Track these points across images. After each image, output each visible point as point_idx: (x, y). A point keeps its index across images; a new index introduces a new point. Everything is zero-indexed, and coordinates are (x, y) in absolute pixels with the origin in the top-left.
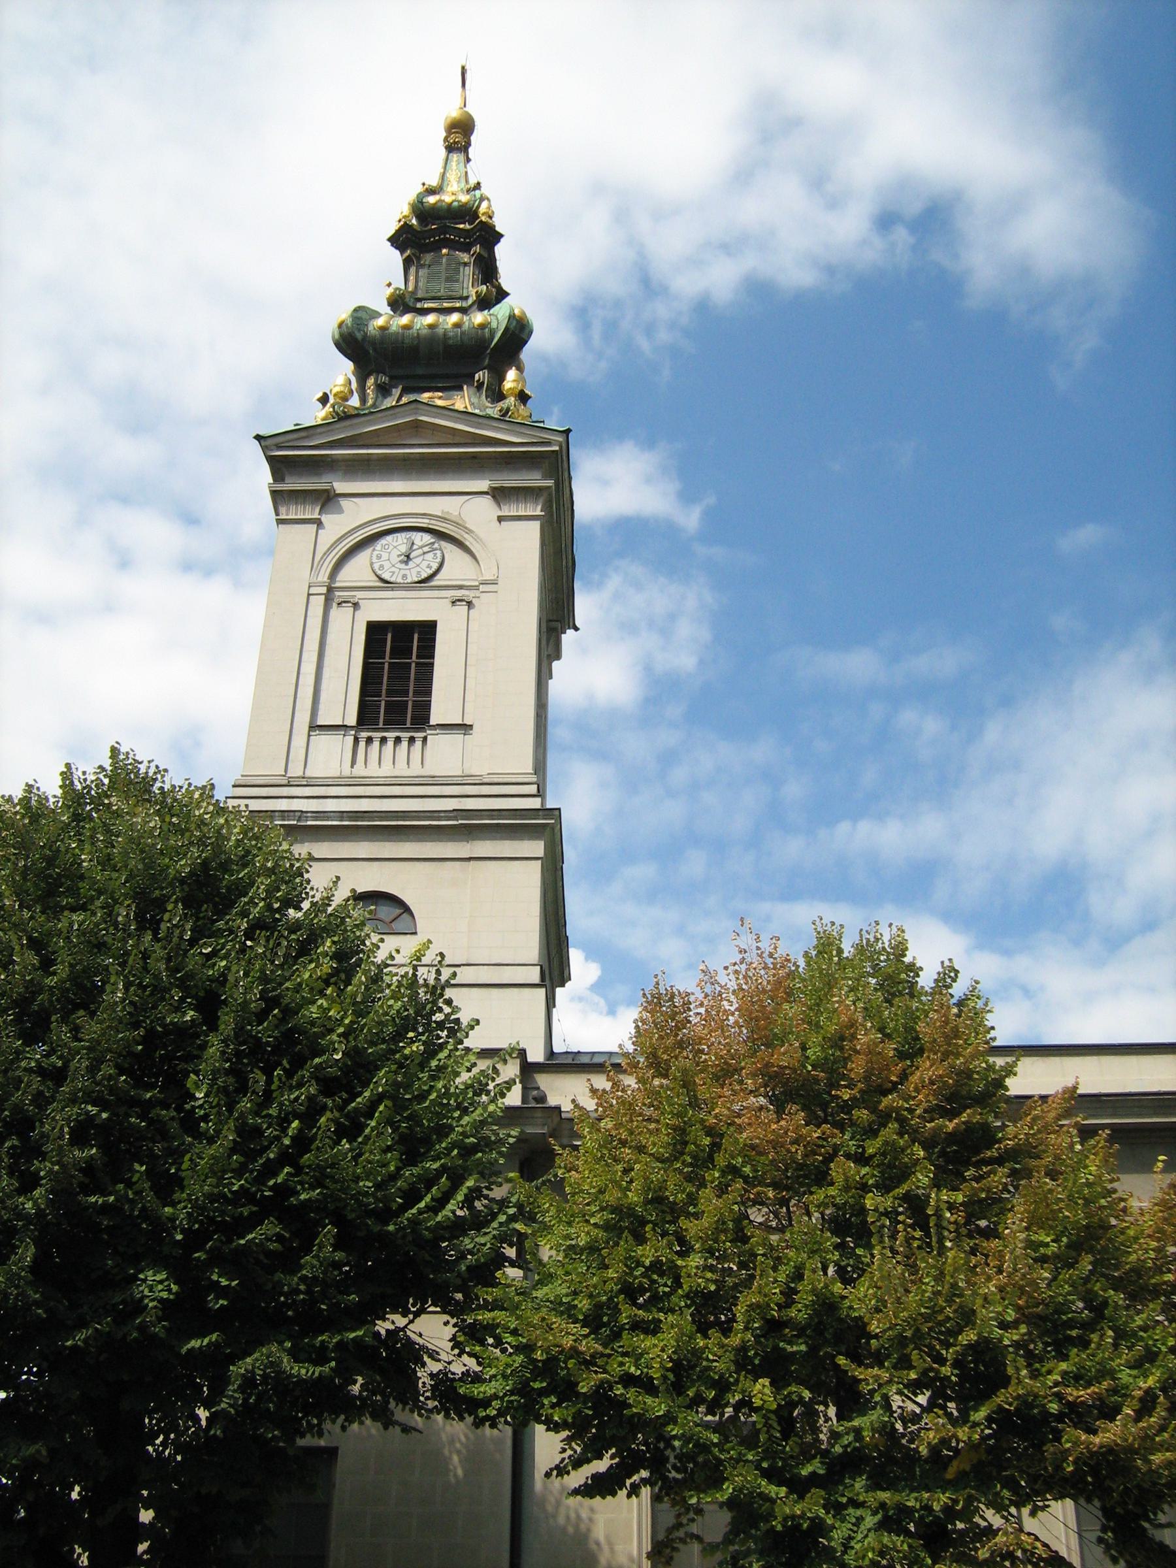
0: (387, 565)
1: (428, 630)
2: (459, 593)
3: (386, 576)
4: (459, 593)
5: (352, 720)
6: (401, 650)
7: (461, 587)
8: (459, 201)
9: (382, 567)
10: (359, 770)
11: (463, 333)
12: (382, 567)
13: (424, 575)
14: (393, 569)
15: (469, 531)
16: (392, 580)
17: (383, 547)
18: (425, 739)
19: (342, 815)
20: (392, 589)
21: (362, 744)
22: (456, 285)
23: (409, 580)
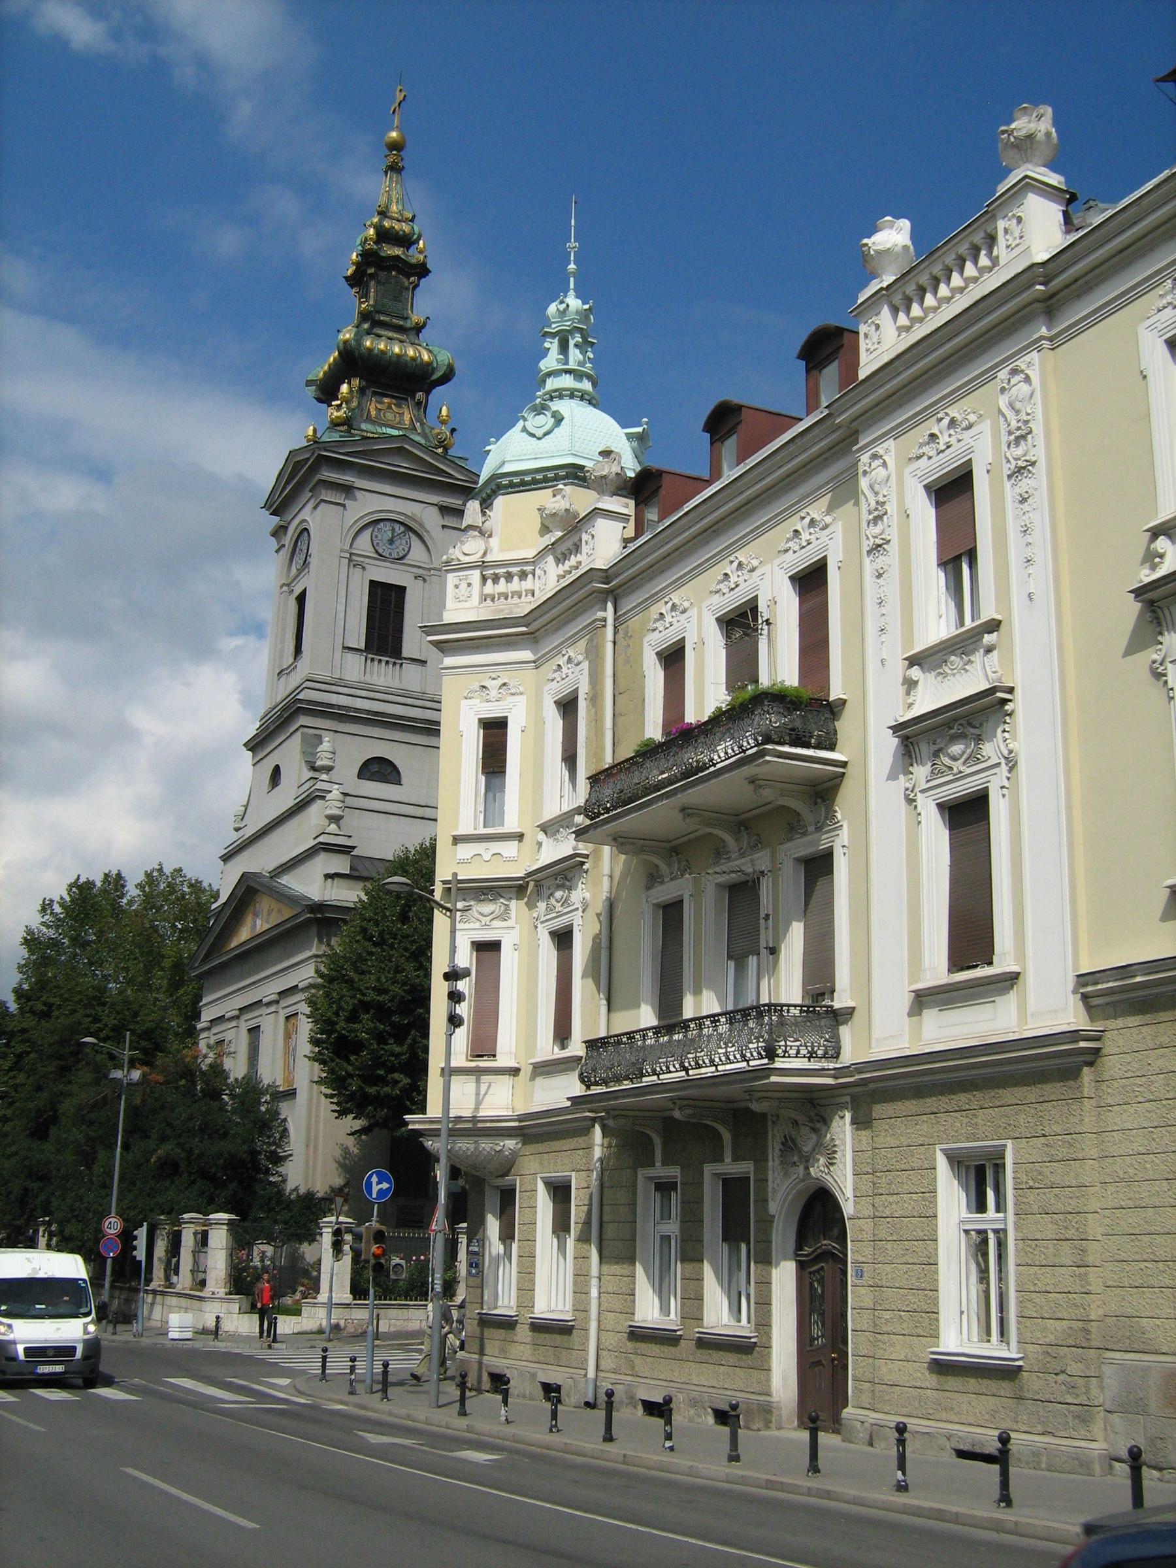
0: (381, 544)
1: (402, 590)
2: (420, 571)
3: (380, 551)
4: (420, 571)
5: (362, 646)
7: (420, 567)
9: (378, 544)
10: (368, 679)
12: (378, 544)
13: (401, 555)
15: (427, 532)
18: (402, 664)
20: (384, 561)
21: (369, 661)
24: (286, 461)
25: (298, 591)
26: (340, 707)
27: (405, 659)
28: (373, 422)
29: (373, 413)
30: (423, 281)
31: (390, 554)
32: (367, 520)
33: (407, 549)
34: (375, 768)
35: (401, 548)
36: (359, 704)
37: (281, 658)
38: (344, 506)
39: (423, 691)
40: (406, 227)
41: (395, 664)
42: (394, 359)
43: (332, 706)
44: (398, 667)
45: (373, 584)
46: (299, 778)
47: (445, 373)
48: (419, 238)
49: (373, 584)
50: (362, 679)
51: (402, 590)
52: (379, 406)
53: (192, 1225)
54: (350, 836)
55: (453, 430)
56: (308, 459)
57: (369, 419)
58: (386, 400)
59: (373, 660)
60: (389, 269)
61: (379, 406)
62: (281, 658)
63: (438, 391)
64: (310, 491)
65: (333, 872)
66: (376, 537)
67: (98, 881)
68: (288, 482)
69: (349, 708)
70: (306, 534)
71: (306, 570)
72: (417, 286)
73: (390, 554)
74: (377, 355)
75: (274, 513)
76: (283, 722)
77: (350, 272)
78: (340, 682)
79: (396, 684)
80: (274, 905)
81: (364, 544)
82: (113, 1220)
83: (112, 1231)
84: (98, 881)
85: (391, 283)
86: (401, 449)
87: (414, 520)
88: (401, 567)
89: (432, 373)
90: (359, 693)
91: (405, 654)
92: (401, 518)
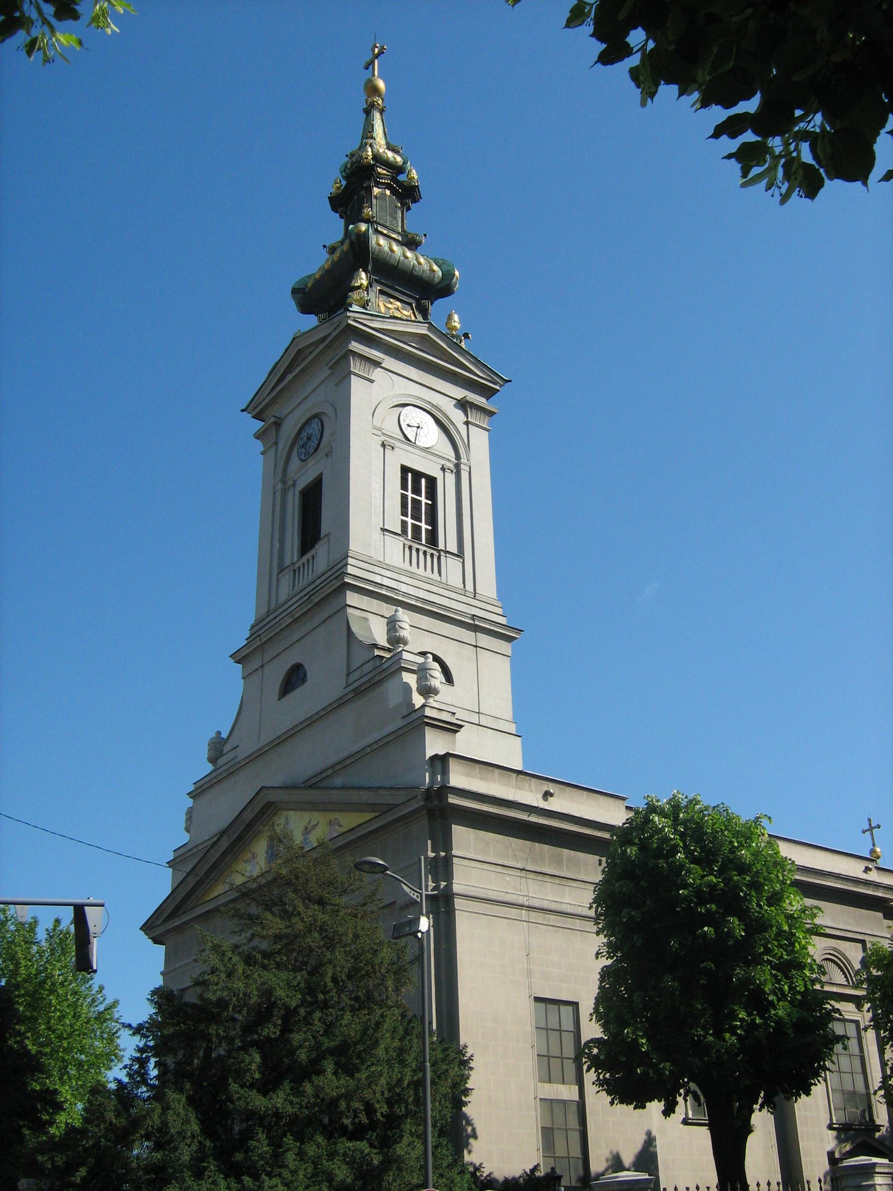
7: (449, 460)
18: (439, 558)
19: (418, 599)
21: (407, 550)
24: (286, 350)
36: (404, 588)
38: (372, 381)
41: (432, 555)
45: (405, 470)
49: (405, 470)
56: (329, 335)
59: (410, 548)
64: (330, 368)
65: (442, 753)
68: (288, 370)
70: (316, 420)
75: (258, 417)
76: (312, 608)
80: (317, 817)
86: (423, 337)
87: (440, 411)
90: (403, 578)
91: (441, 546)
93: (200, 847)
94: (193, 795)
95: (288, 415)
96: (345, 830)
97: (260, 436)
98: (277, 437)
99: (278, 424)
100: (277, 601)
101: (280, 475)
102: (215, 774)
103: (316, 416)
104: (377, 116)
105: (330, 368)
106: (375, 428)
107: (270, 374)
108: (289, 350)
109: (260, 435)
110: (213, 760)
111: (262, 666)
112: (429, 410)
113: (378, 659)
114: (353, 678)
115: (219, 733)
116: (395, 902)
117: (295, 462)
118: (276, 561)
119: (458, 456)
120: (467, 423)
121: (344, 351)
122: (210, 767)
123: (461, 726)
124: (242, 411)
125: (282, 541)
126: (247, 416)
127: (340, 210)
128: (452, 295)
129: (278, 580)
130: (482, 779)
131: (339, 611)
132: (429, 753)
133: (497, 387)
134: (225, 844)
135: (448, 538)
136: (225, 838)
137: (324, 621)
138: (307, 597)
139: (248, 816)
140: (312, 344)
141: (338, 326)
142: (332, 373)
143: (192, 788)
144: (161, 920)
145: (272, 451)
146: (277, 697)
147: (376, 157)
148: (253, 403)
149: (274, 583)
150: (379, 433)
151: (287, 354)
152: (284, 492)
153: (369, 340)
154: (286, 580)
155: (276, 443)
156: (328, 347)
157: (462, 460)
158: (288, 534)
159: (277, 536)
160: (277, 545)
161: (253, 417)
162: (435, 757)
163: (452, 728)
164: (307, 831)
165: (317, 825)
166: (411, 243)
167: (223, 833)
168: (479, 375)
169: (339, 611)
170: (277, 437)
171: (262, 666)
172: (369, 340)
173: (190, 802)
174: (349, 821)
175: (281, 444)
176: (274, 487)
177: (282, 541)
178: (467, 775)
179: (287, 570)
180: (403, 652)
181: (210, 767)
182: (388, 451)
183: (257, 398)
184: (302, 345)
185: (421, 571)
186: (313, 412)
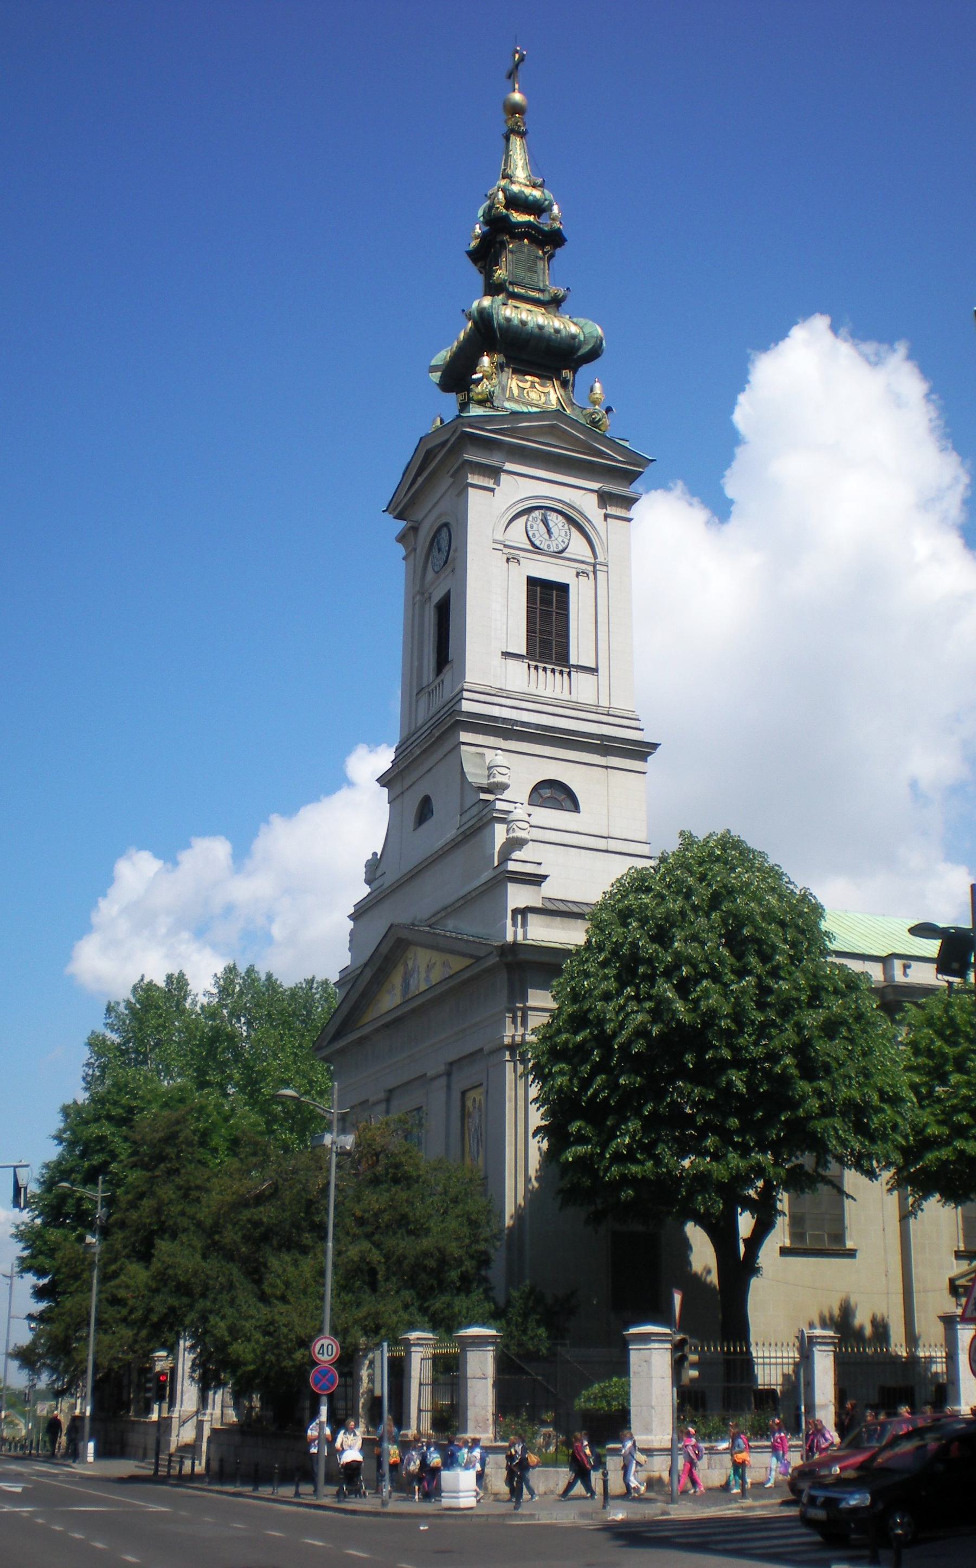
0: (537, 535)
1: (563, 589)
3: (537, 543)
5: (524, 652)
6: (546, 601)
7: (583, 562)
8: (535, 197)
11: (561, 338)
12: (534, 535)
13: (561, 548)
14: (541, 539)
15: (589, 521)
16: (541, 547)
17: (533, 518)
18: (569, 674)
19: (538, 726)
20: (541, 554)
21: (532, 669)
22: (535, 276)
23: (552, 550)
24: (416, 450)
25: (437, 596)
26: (505, 720)
27: (573, 666)
28: (517, 401)
29: (516, 392)
30: (558, 251)
31: (549, 546)
32: (520, 507)
33: (566, 542)
34: (547, 793)
35: (560, 539)
37: (420, 676)
39: (596, 704)
40: (537, 193)
42: (536, 330)
43: (495, 719)
44: (565, 676)
45: (532, 582)
46: (462, 805)
47: (594, 346)
48: (551, 205)
49: (532, 582)
50: (526, 690)
51: (563, 589)
52: (521, 384)
53: (420, 1349)
54: (540, 864)
55: (609, 410)
56: (447, 441)
57: (511, 399)
58: (528, 378)
59: (536, 668)
60: (521, 237)
61: (521, 384)
62: (420, 676)
63: (584, 369)
64: (452, 476)
65: (522, 906)
66: (532, 527)
67: (161, 982)
68: (418, 474)
69: (516, 722)
70: (445, 530)
71: (449, 570)
72: (551, 257)
73: (549, 546)
74: (517, 326)
75: (399, 517)
76: (434, 742)
77: (474, 244)
78: (501, 693)
79: (567, 697)
80: (436, 957)
81: (517, 535)
82: (326, 1342)
83: (326, 1358)
84: (161, 982)
85: (523, 252)
86: (553, 427)
88: (561, 562)
89: (579, 348)
91: (573, 661)
92: (559, 506)
93: (353, 975)
94: (353, 917)
95: (423, 519)
96: (452, 972)
97: (401, 538)
98: (415, 543)
99: (414, 529)
100: (416, 724)
101: (417, 588)
102: (371, 897)
103: (446, 525)
104: (517, 144)
105: (452, 476)
106: (495, 542)
107: (404, 475)
108: (419, 450)
109: (401, 538)
110: (368, 882)
111: (403, 793)
112: (560, 509)
113: (481, 805)
114: (467, 817)
115: (375, 854)
116: (481, 1050)
117: (430, 574)
118: (415, 680)
119: (595, 557)
120: (606, 516)
121: (460, 461)
122: (366, 890)
123: (545, 877)
124: (384, 511)
125: (420, 659)
126: (389, 517)
127: (479, 264)
128: (600, 358)
129: (417, 702)
130: (563, 929)
131: (453, 749)
132: (511, 905)
133: (641, 470)
134: (368, 974)
135: (579, 652)
136: (368, 969)
137: (445, 756)
138: (429, 731)
139: (385, 949)
140: (437, 446)
141: (454, 432)
142: (454, 482)
143: (352, 910)
144: (327, 1041)
145: (412, 556)
146: (412, 826)
147: (515, 202)
148: (392, 505)
149: (414, 702)
150: (501, 547)
151: (416, 454)
152: (422, 608)
153: (488, 445)
154: (424, 699)
155: (415, 550)
156: (450, 451)
157: (598, 560)
158: (426, 650)
159: (416, 654)
160: (416, 664)
161: (395, 518)
162: (516, 912)
163: (536, 880)
164: (429, 968)
165: (435, 963)
166: (554, 304)
167: (366, 965)
168: (619, 460)
169: (453, 749)
170: (415, 543)
171: (403, 793)
172: (488, 445)
173: (351, 924)
174: (458, 964)
175: (418, 550)
176: (414, 598)
177: (420, 659)
178: (548, 926)
179: (423, 692)
180: (497, 802)
181: (366, 890)
182: (513, 564)
183: (395, 499)
184: (430, 445)
185: (548, 693)
186: (444, 520)
